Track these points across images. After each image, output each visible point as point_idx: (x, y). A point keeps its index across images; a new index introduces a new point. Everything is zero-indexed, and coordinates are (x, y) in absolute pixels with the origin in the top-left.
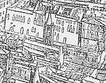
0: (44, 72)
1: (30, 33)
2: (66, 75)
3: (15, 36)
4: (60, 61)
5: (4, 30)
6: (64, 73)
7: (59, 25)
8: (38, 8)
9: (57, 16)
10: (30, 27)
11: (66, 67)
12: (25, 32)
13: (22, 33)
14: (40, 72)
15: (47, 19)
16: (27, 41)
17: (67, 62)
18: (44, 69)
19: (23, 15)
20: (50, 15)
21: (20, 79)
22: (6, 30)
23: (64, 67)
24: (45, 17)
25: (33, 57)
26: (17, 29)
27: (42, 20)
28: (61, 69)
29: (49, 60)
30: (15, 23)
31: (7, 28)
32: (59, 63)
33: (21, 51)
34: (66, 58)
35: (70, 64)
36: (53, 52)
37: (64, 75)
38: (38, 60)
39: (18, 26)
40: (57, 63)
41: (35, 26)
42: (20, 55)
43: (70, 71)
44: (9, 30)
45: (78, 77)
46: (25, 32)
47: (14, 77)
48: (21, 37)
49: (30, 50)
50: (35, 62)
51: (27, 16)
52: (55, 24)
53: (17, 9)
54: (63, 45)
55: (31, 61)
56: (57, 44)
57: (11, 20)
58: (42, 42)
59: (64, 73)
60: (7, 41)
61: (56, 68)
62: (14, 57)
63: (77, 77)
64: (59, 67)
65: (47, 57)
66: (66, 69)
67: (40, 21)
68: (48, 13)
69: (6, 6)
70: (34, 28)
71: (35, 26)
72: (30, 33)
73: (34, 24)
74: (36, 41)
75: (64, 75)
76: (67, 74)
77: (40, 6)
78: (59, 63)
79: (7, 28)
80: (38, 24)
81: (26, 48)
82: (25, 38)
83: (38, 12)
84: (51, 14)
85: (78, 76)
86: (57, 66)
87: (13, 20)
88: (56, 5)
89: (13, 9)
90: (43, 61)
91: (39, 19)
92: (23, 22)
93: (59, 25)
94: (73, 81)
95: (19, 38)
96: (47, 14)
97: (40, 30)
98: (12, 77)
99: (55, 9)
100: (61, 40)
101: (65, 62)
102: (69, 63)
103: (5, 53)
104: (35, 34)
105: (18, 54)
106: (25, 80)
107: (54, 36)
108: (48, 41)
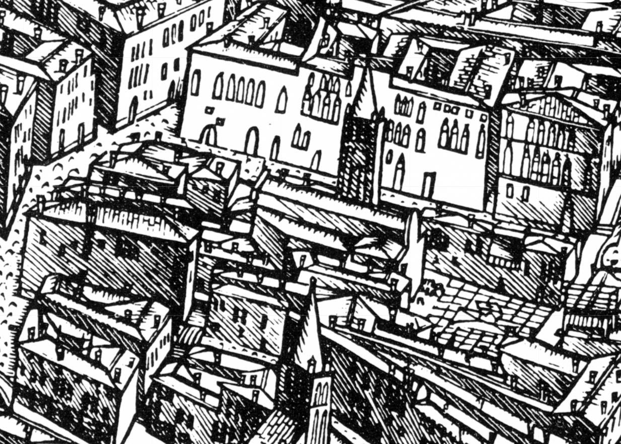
0: (340, 322)
1: (287, 153)
2: (432, 333)
3: (223, 164)
4: (407, 274)
5: (177, 141)
6: (422, 323)
7: (404, 121)
8: (320, 47)
9: (397, 82)
10: (284, 127)
11: (435, 298)
12: (265, 150)
13: (250, 150)
14: (325, 321)
15: (354, 93)
16: (271, 187)
17: (439, 279)
18: (340, 307)
19: (259, 74)
20: (368, 77)
21: (239, 350)
22: (183, 140)
23: (427, 299)
24: (349, 84)
25: (297, 256)
26: (230, 138)
27: (338, 99)
28: (415, 308)
29: (363, 269)
30: (223, 108)
31: (191, 131)
32: (402, 284)
33: (245, 228)
34: (431, 261)
35: (448, 285)
36: (383, 236)
37: (425, 335)
38: (315, 268)
39: (238, 119)
40: (397, 281)
41: (308, 124)
42: (244, 245)
43: (449, 315)
44: (197, 138)
45: (480, 344)
46: (265, 150)
47: (215, 343)
48: (247, 171)
49: (286, 227)
50: (304, 277)
51: (275, 81)
52: (389, 115)
53: (234, 51)
54: (421, 204)
55: (290, 272)
56: (397, 200)
57: (205, 97)
58: (337, 194)
59: (422, 323)
60: (190, 187)
61: (393, 302)
62: (217, 253)
63: (480, 340)
64: (405, 297)
65: (356, 258)
66: (435, 308)
67: (327, 101)
68: (361, 66)
69: (190, 37)
70: (303, 131)
71: (308, 124)
72: (287, 153)
73: (302, 113)
74: (308, 186)
75: (425, 335)
76: (437, 330)
77: (328, 39)
78: (402, 284)
79: (191, 131)
80: (319, 116)
81: (273, 220)
82: (266, 173)
83: (320, 63)
84: (375, 73)
85: (485, 339)
86: (398, 295)
87: (217, 94)
88: (392, 34)
89: (219, 49)
90: (339, 274)
91: (323, 94)
92: (259, 103)
93: (404, 121)
94: (460, 358)
95: (239, 174)
96: (358, 72)
97: (328, 139)
98: (206, 341)
99: (390, 50)
100: (413, 183)
101: (429, 275)
102: (444, 280)
103: (176, 238)
104: (304, 158)
105: (236, 241)
106: (260, 356)
107: (385, 165)
108: (358, 187)
